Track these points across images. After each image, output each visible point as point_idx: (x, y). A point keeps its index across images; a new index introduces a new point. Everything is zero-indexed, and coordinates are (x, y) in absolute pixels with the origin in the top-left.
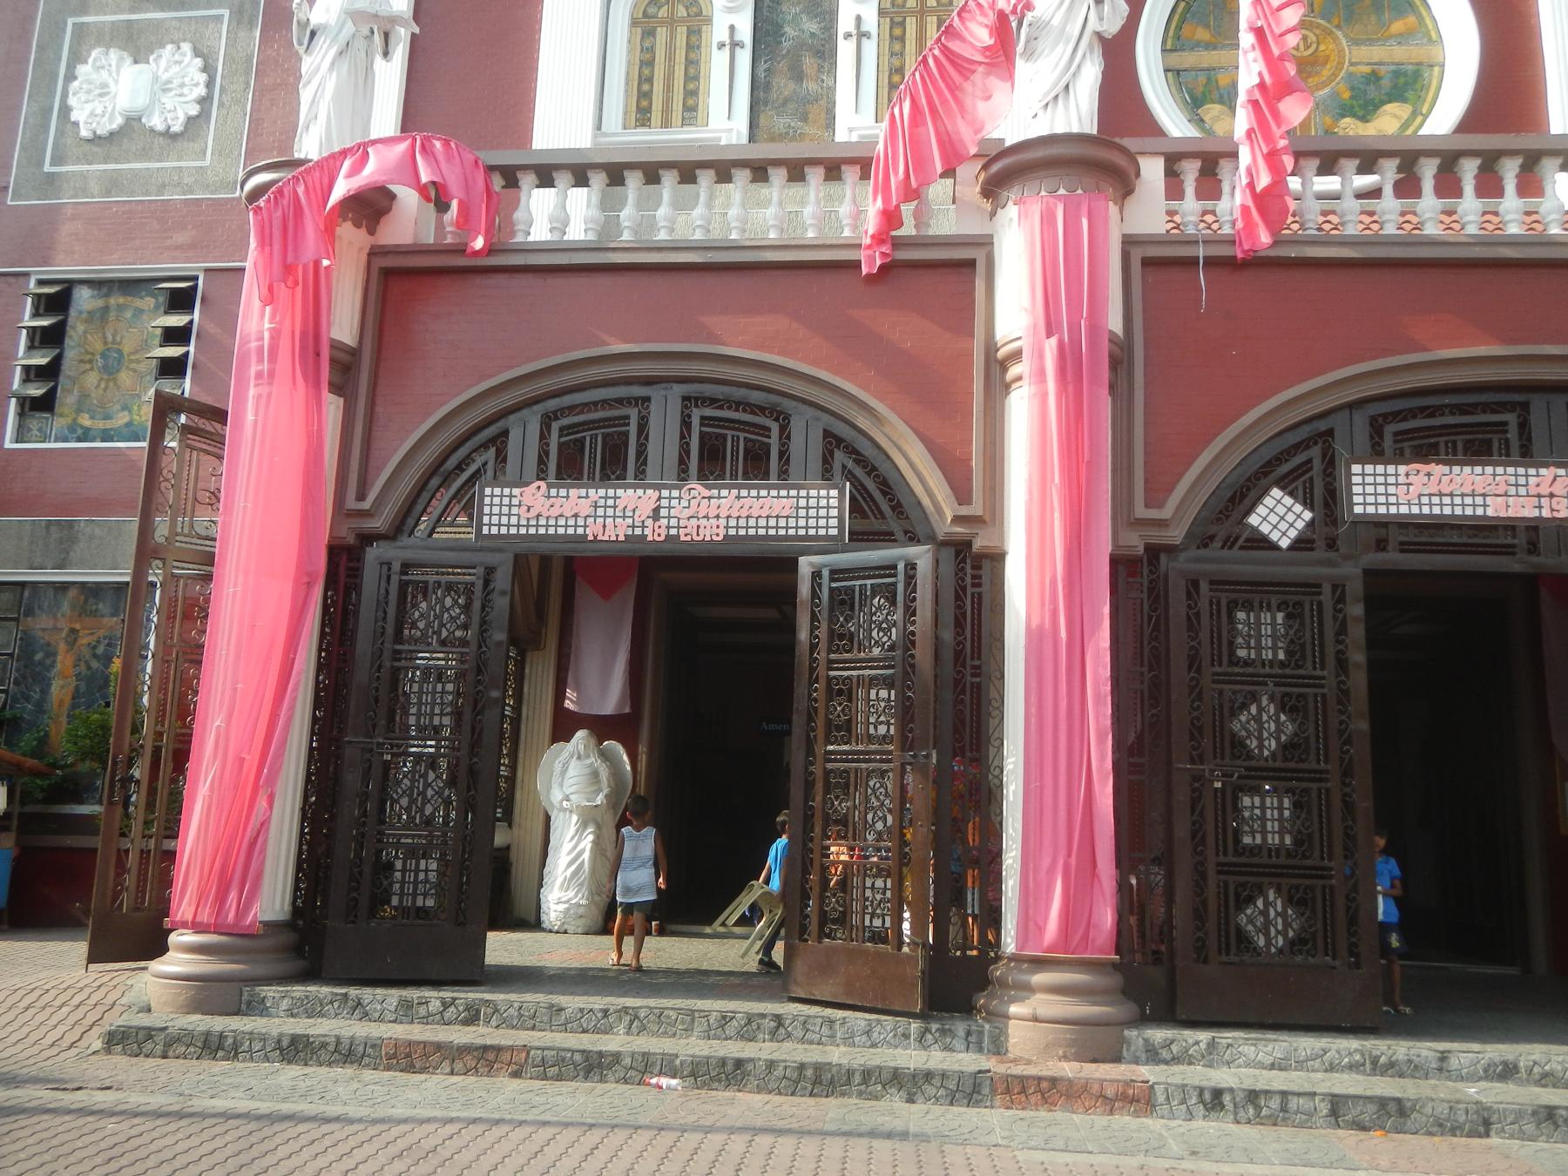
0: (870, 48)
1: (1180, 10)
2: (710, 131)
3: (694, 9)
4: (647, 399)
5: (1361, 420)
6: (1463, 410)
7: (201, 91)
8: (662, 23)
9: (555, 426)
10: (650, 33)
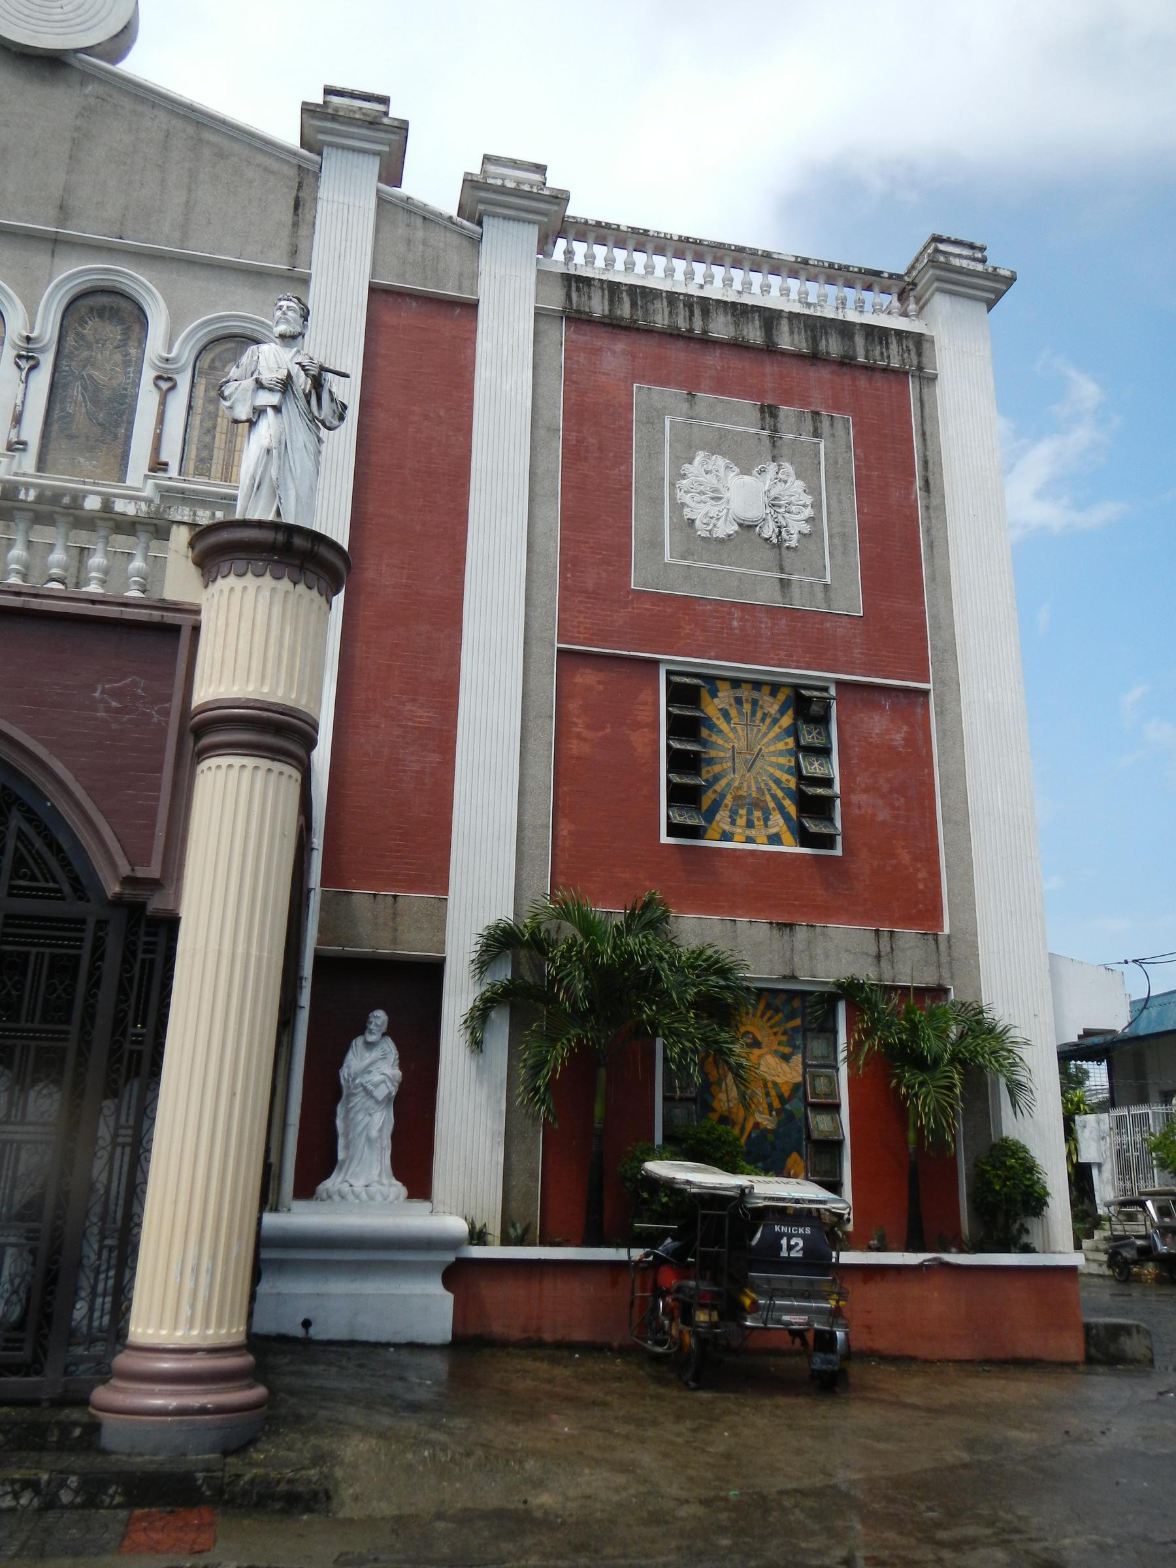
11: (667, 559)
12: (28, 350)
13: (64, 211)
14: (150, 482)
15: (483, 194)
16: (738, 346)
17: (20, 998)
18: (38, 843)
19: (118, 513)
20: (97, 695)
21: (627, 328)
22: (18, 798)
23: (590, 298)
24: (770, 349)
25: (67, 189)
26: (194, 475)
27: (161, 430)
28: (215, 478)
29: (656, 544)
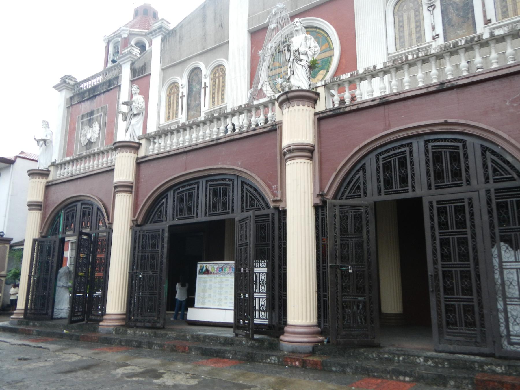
5: (172, 192)
6: (189, 185)
7: (98, 132)
8: (172, 94)
9: (176, 192)
10: (170, 97)
12: (431, 3)
14: (487, 29)
17: (509, 218)
18: (499, 162)
19: (497, 36)
20: (508, 104)
22: (487, 148)
26: (502, 19)
27: (485, 8)
28: (511, 17)
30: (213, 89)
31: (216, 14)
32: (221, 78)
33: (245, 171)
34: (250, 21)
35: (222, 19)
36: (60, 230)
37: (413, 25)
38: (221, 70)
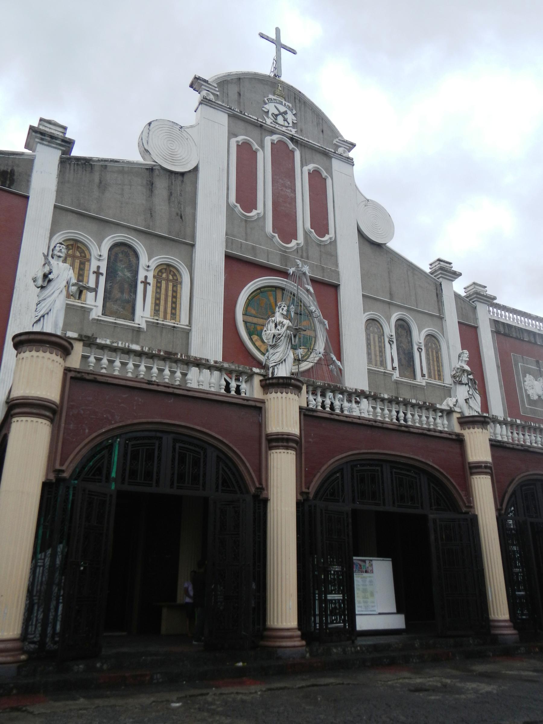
0: (150, 289)
1: (247, 302)
2: (88, 305)
3: (83, 255)
4: (161, 438)
6: (371, 465)
11: (527, 406)
12: (391, 338)
13: (391, 296)
15: (478, 296)
16: (529, 342)
21: (507, 336)
23: (500, 327)
24: (535, 343)
25: (390, 288)
29: (523, 401)
30: (157, 292)
31: (171, 194)
32: (171, 284)
33: (441, 470)
34: (229, 241)
35: (182, 208)
36: (113, 475)
37: (377, 348)
38: (172, 273)
